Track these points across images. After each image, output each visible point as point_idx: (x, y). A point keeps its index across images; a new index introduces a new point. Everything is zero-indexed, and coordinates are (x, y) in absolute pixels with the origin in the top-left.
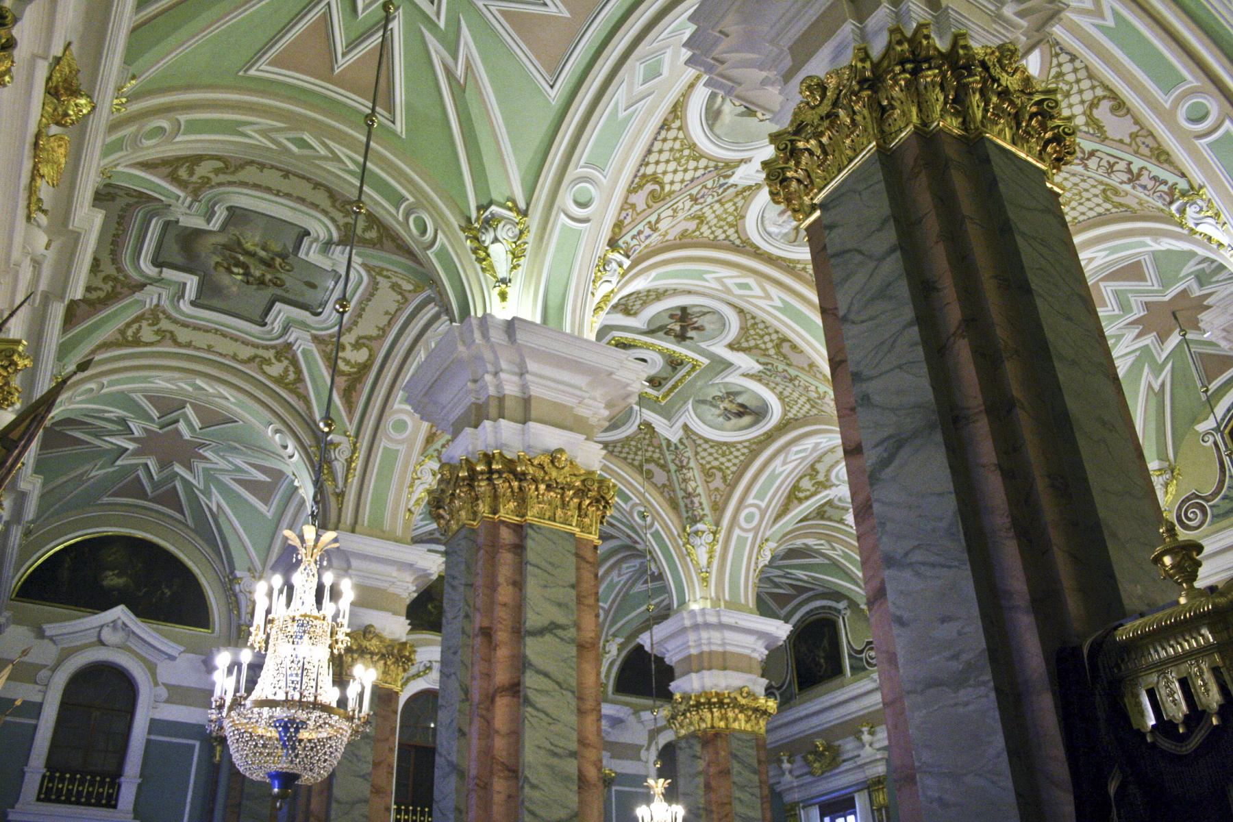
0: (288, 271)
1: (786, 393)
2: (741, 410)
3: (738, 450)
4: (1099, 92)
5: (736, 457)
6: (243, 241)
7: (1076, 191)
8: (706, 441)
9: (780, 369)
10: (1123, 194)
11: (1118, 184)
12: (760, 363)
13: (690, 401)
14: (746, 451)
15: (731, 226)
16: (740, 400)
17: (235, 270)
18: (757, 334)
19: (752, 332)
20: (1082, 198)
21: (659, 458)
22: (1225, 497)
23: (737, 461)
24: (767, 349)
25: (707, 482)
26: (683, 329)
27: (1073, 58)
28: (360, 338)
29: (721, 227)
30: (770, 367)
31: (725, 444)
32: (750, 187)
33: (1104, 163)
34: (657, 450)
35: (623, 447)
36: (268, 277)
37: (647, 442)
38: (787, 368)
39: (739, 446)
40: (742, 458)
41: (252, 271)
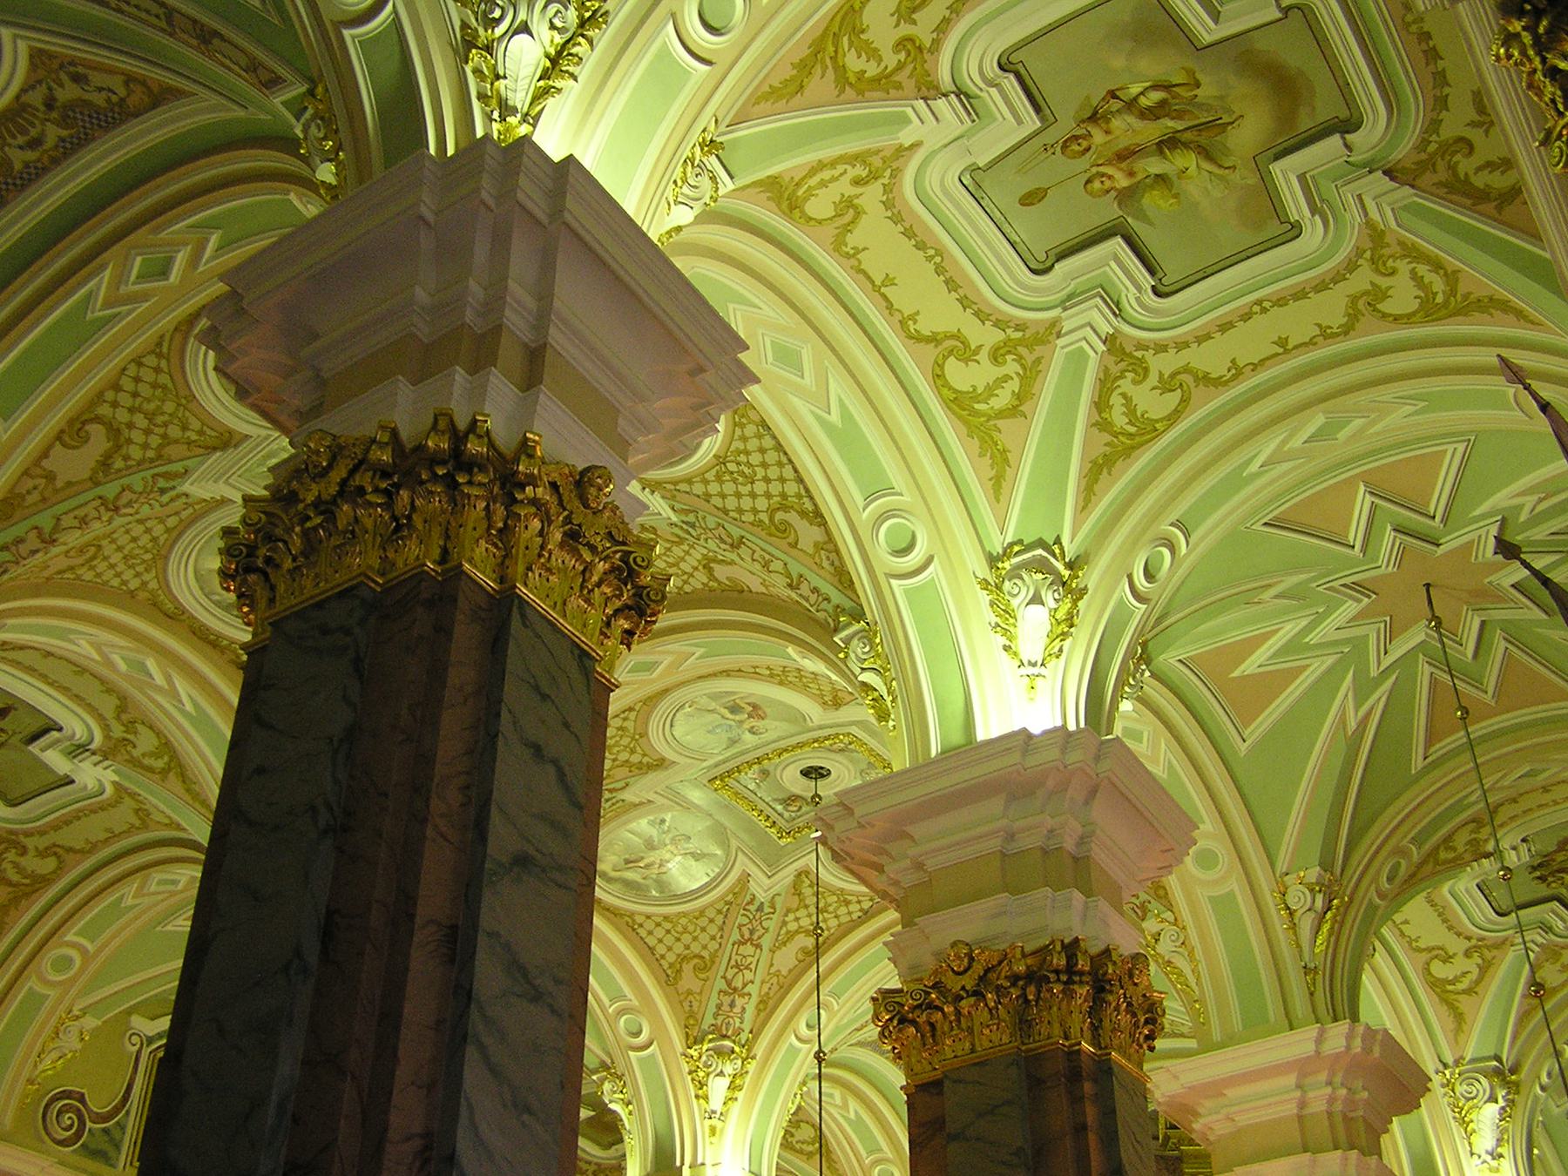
0: (1088, 181)
6: (1206, 165)
7: (691, 928)
10: (702, 976)
11: (721, 973)
17: (1156, 96)
20: (682, 933)
21: (126, 458)
22: (106, 1131)
28: (858, 213)
33: (749, 959)
34: (151, 454)
35: (155, 386)
36: (1098, 137)
37: (174, 432)
41: (1131, 119)
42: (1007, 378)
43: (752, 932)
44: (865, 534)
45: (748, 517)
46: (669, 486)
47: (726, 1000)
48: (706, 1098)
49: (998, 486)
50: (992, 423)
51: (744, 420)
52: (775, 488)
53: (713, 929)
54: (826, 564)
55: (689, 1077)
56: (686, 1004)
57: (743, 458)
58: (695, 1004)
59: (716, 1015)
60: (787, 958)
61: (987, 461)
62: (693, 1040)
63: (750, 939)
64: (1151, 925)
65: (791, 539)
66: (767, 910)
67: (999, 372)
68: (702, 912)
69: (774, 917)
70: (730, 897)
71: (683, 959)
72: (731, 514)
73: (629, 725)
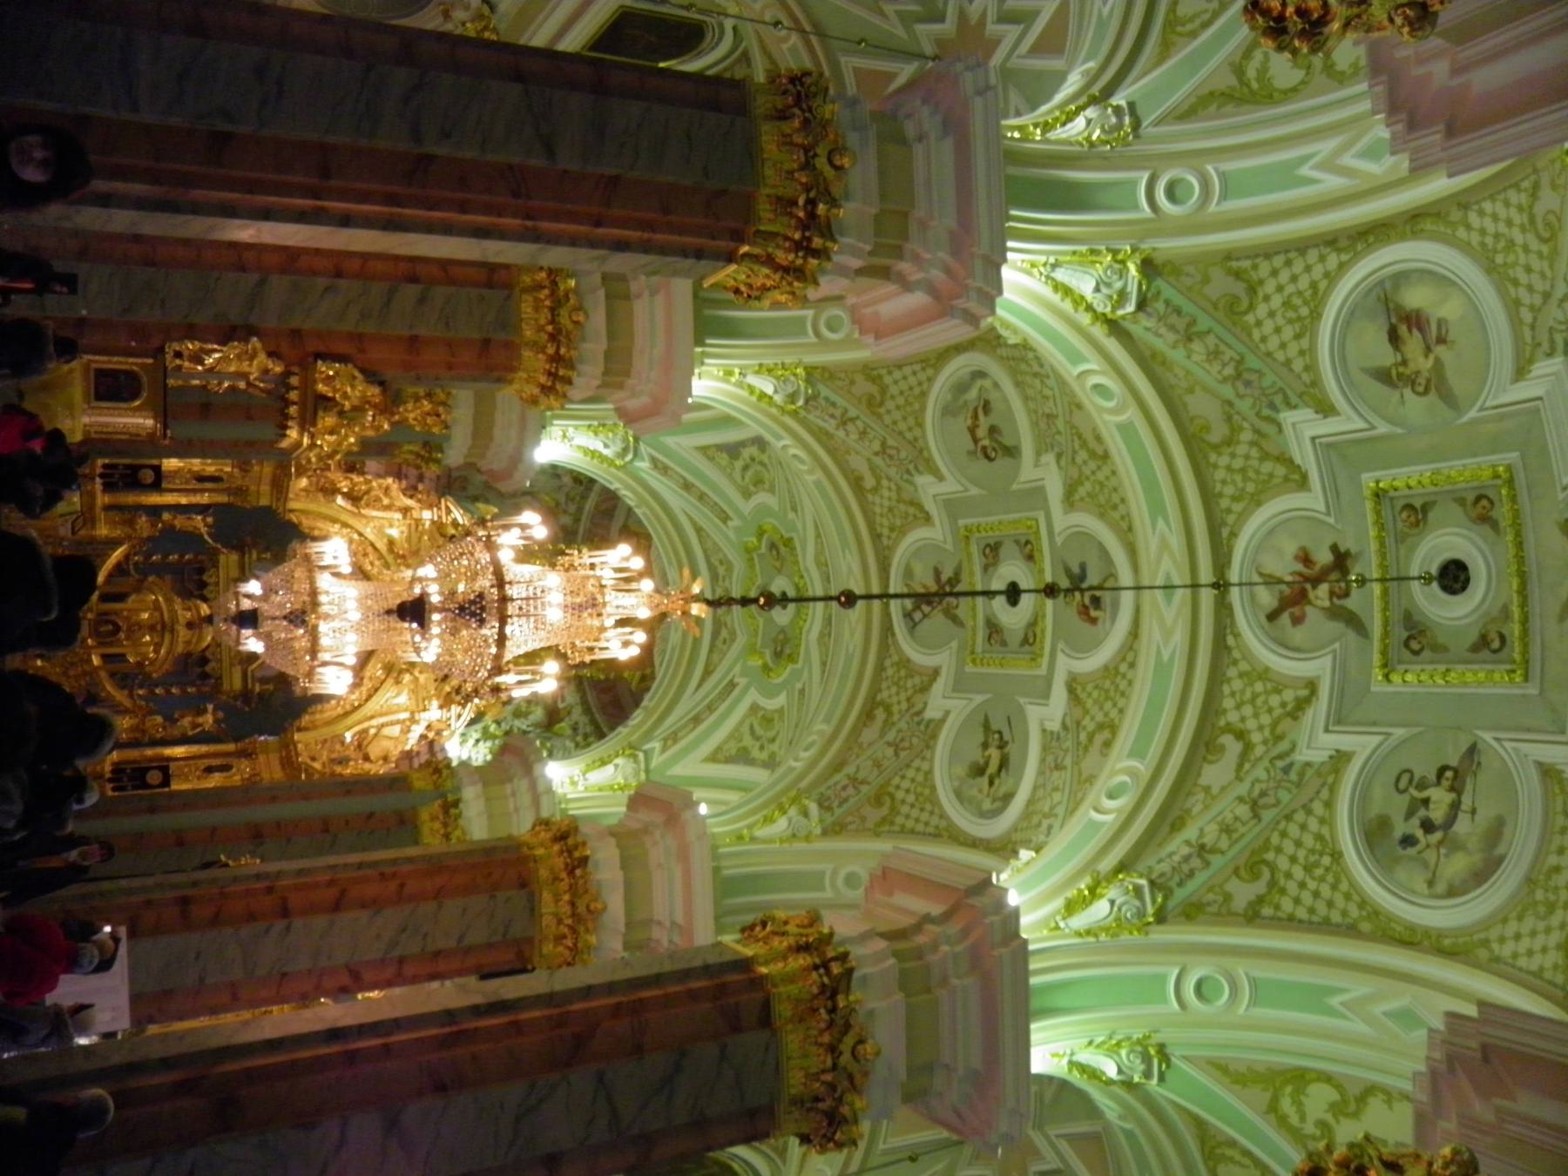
1: (1288, 332)
2: (1403, 329)
3: (1483, 232)
4: (870, 497)
5: (1495, 218)
7: (909, 409)
8: (1513, 306)
9: (1248, 402)
11: (862, 416)
12: (1279, 426)
13: (1465, 419)
14: (1473, 218)
15: (1117, 671)
16: (1386, 356)
18: (1246, 479)
19: (1250, 488)
23: (1500, 208)
24: (1253, 444)
25: (1559, 220)
26: (1316, 581)
27: (876, 537)
29: (1117, 686)
30: (1266, 412)
31: (1490, 269)
32: (1071, 690)
38: (1237, 402)
39: (1475, 238)
40: (1487, 206)
42: (1303, 1118)
43: (891, 457)
44: (1228, 962)
45: (1275, 839)
46: (1330, 779)
47: (838, 413)
48: (757, 373)
49: (1220, 1068)
50: (1272, 1089)
51: (1364, 913)
52: (1292, 887)
53: (902, 426)
54: (1211, 896)
55: (779, 362)
56: (843, 375)
57: (1330, 878)
58: (840, 383)
59: (827, 399)
60: (859, 464)
61: (1243, 1069)
62: (811, 371)
63: (884, 452)
64: (813, 808)
65: (1243, 873)
66: (905, 477)
67: (1310, 1119)
68: (921, 425)
69: (898, 477)
70: (925, 453)
71: (884, 390)
72: (1283, 823)
73: (1116, 515)
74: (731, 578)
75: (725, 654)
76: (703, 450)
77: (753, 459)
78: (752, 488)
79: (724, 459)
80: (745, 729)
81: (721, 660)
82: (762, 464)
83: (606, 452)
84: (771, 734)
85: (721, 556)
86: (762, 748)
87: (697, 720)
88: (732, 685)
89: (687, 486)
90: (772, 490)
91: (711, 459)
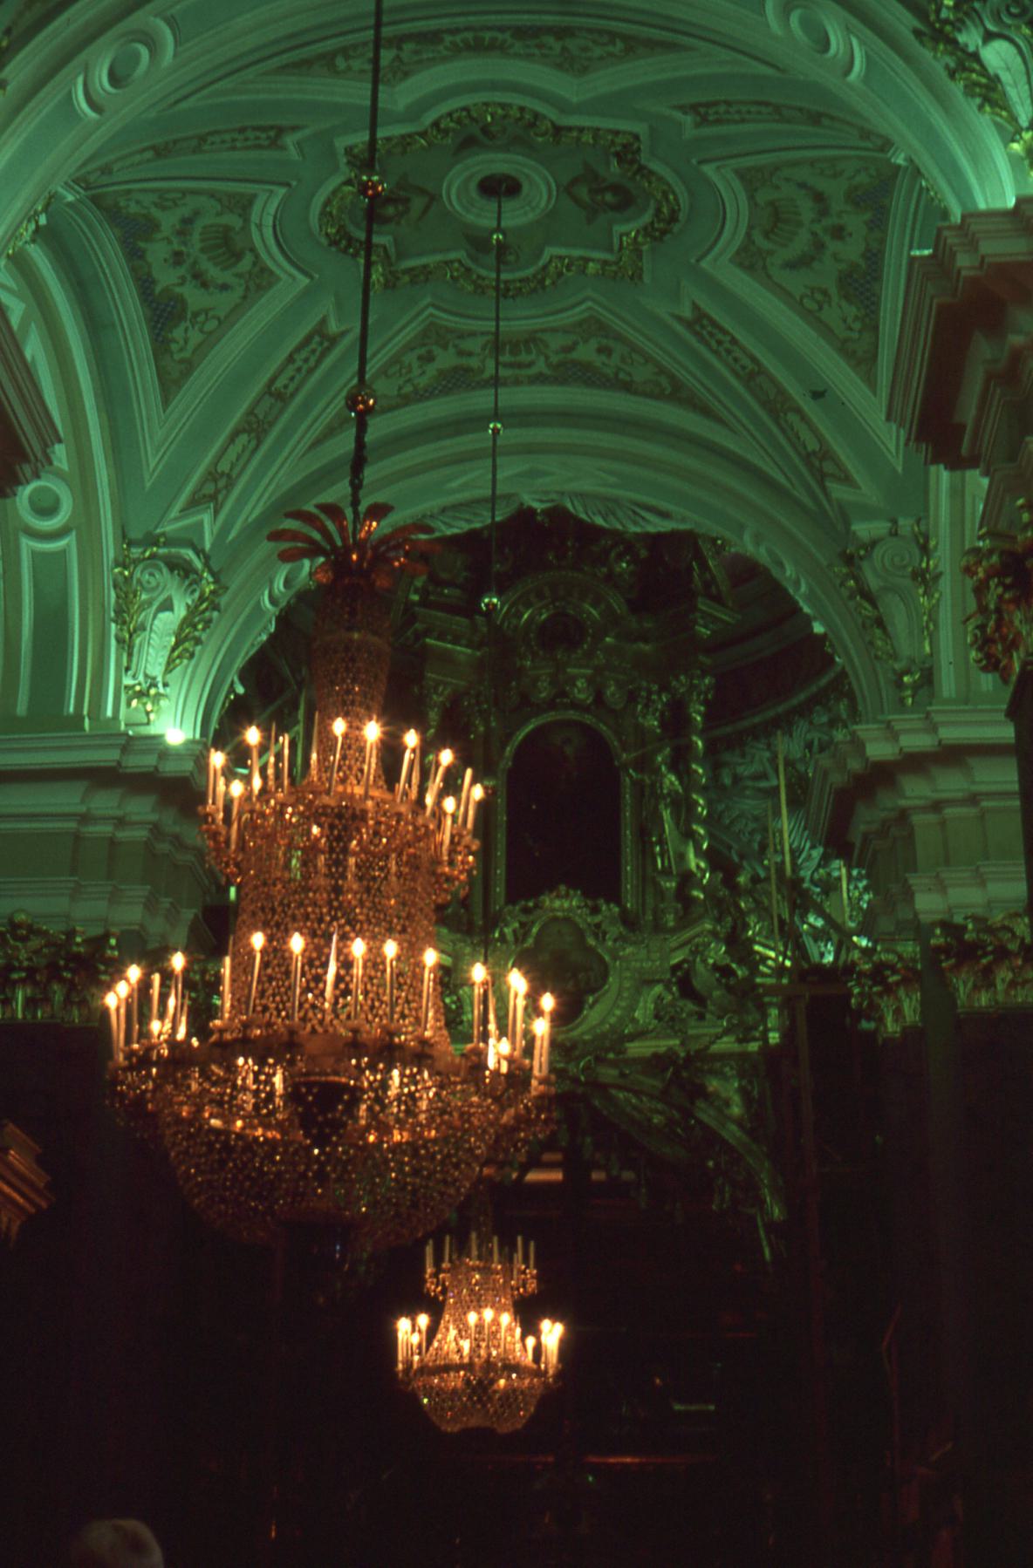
74: (462, 336)
75: (634, 348)
76: (169, 386)
77: (178, 258)
78: (246, 263)
79: (184, 336)
80: (797, 282)
81: (648, 359)
82: (183, 232)
83: (180, 611)
84: (807, 209)
85: (411, 358)
86: (838, 232)
87: (778, 405)
88: (699, 322)
89: (255, 427)
90: (244, 205)
91: (189, 367)
